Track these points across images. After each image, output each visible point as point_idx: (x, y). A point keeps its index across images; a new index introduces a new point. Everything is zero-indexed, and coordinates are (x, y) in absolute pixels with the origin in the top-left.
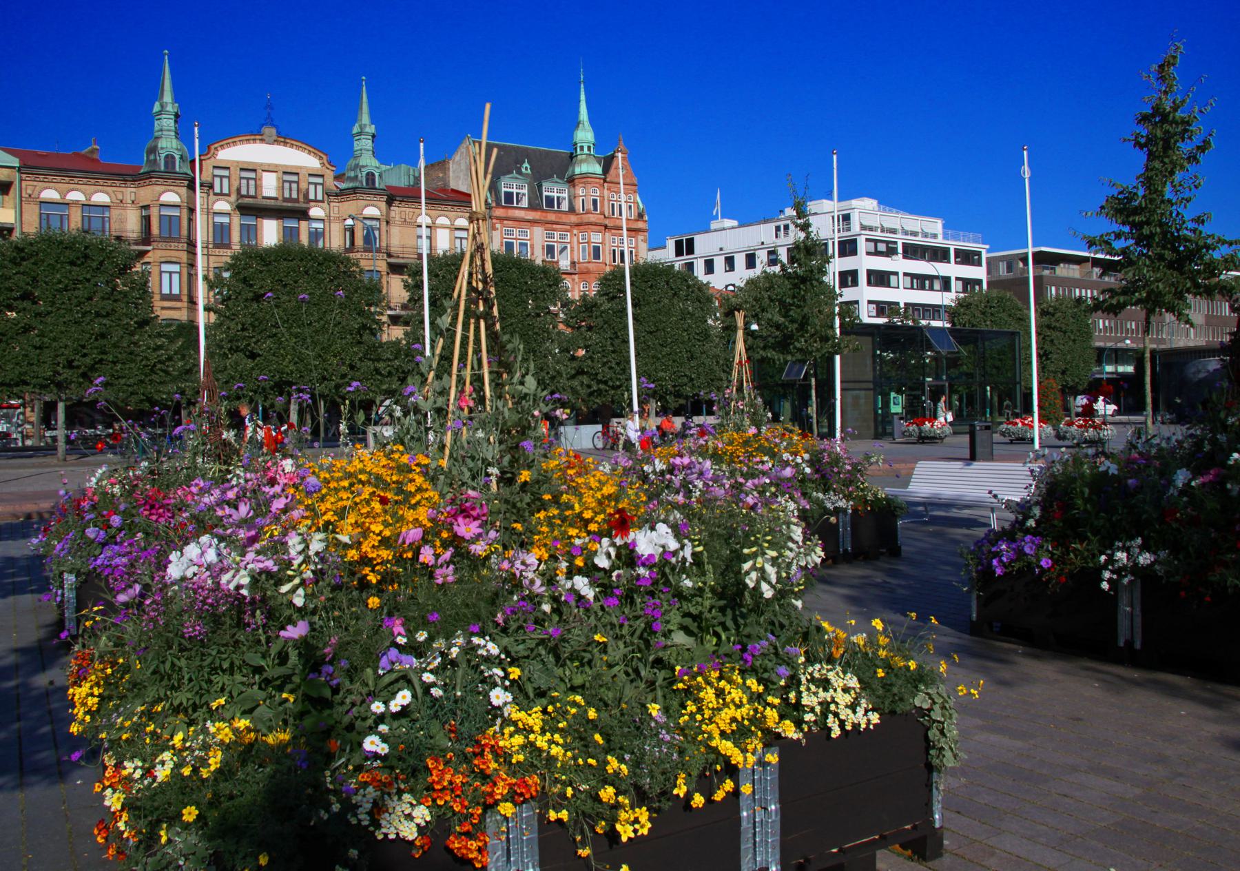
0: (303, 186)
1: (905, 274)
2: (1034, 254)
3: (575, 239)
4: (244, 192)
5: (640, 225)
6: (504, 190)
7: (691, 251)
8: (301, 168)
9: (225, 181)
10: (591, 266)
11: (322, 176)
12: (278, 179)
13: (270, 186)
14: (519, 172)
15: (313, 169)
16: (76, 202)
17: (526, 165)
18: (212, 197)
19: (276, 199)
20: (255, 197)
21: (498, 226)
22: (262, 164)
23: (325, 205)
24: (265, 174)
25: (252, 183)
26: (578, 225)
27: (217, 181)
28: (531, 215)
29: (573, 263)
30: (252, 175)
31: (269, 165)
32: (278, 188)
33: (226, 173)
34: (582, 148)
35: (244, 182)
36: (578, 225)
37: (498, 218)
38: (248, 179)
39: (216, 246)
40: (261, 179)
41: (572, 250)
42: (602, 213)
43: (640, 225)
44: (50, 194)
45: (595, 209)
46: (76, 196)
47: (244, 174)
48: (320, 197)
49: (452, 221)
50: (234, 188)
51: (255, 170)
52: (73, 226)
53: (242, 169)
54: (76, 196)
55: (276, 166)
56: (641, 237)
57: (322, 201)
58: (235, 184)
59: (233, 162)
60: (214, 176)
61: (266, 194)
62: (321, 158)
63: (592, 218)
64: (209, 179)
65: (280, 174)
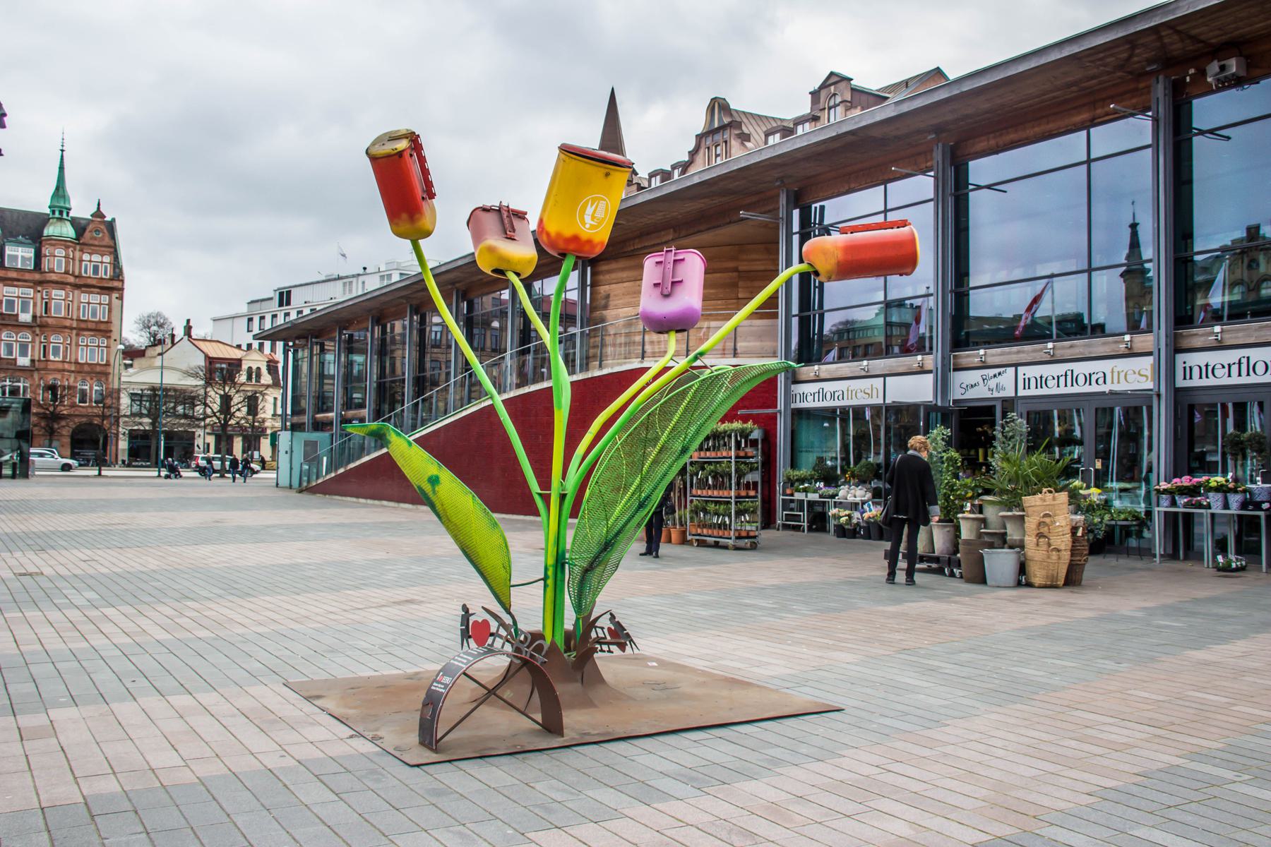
5: (116, 284)
7: (288, 303)
10: (50, 321)
26: (41, 283)
34: (54, 212)
36: (41, 283)
41: (35, 305)
43: (116, 284)
56: (115, 295)
63: (54, 277)
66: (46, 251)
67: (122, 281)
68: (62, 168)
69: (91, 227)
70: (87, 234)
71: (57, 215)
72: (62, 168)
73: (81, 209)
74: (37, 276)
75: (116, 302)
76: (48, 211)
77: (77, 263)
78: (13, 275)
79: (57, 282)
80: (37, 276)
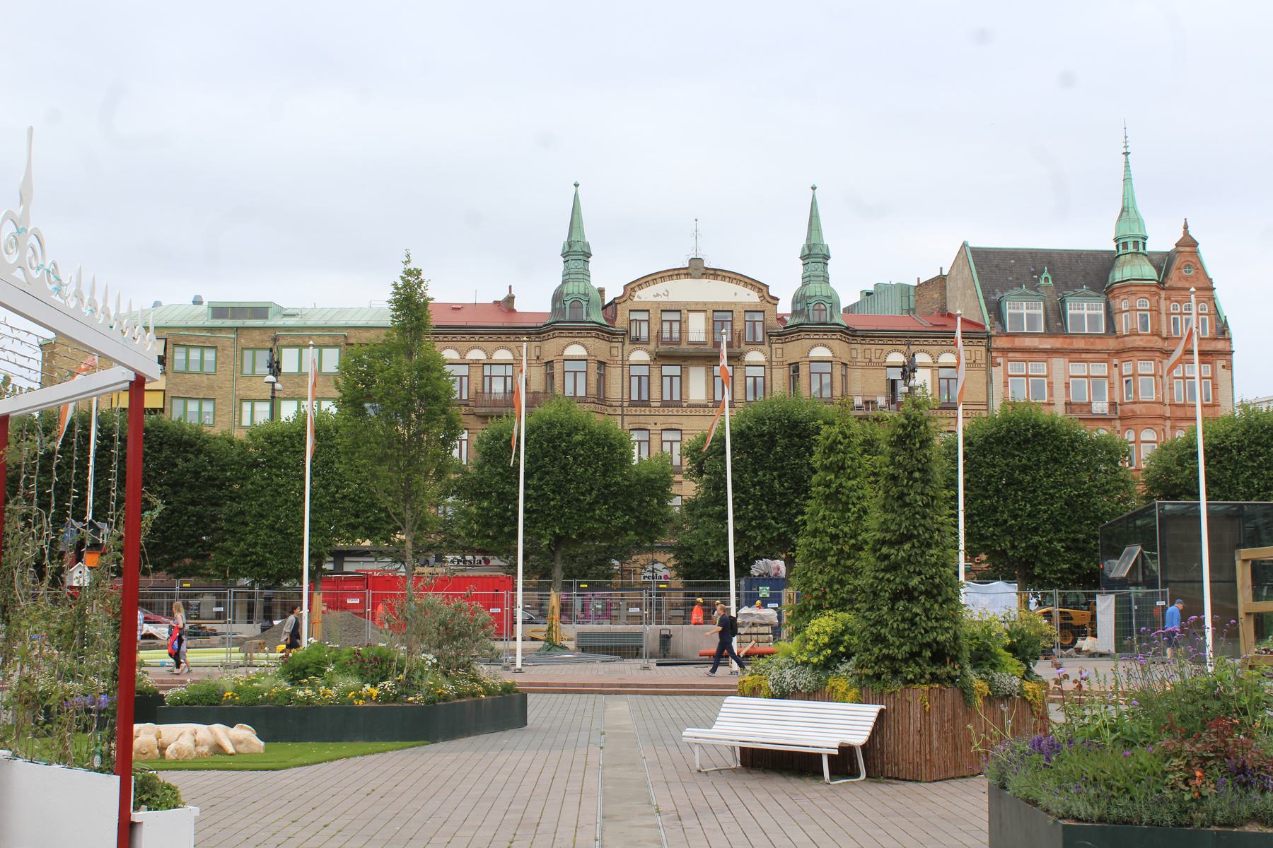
0: (739, 326)
2: (1089, 316)
3: (1116, 370)
4: (666, 335)
6: (1008, 311)
8: (735, 304)
9: (644, 326)
10: (1137, 408)
12: (707, 319)
13: (697, 329)
14: (1034, 286)
15: (750, 304)
17: (1046, 274)
18: (628, 347)
19: (704, 343)
20: (676, 343)
21: (1000, 360)
22: (688, 303)
23: (766, 348)
24: (691, 315)
25: (676, 326)
26: (1118, 352)
28: (1048, 344)
29: (1113, 405)
30: (676, 316)
31: (696, 303)
32: (707, 333)
33: (644, 316)
34: (1125, 245)
35: (666, 326)
36: (1118, 352)
37: (997, 349)
38: (671, 322)
39: (633, 404)
40: (686, 321)
42: (1157, 334)
43: (1220, 345)
45: (1145, 327)
47: (666, 316)
48: (760, 339)
49: (935, 358)
50: (654, 334)
52: (472, 388)
55: (705, 304)
56: (1220, 363)
57: (762, 343)
58: (655, 328)
61: (691, 339)
62: (760, 290)
63: (1138, 342)
64: (625, 325)
65: (710, 314)
66: (1122, 304)
67: (1230, 339)
68: (1127, 179)
69: (1177, 263)
70: (1174, 274)
71: (1131, 248)
72: (1127, 179)
73: (1162, 240)
74: (1112, 344)
75: (1222, 373)
76: (1112, 247)
77: (1164, 317)
78: (1080, 344)
79: (1144, 350)
80: (1112, 344)
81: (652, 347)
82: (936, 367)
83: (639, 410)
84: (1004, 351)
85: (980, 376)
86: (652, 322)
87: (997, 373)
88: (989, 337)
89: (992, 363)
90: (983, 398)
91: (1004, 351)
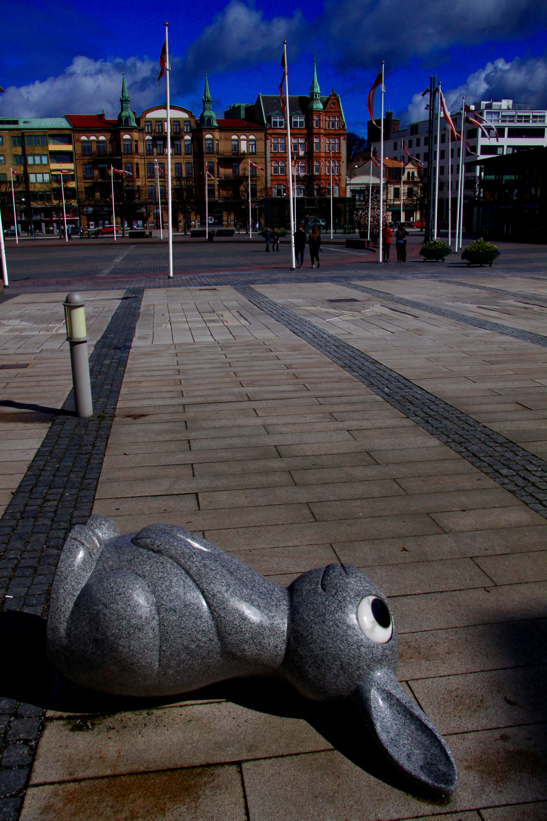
0: (182, 126)
1: (508, 147)
11: (190, 121)
16: (94, 140)
21: (269, 137)
27: (146, 127)
39: (147, 155)
44: (84, 138)
46: (93, 138)
51: (162, 121)
53: (156, 121)
54: (93, 138)
57: (189, 132)
59: (153, 118)
60: (145, 125)
62: (188, 114)
77: (324, 122)
81: (153, 134)
82: (248, 140)
83: (188, 156)
84: (271, 134)
85: (263, 143)
86: (153, 125)
87: (268, 142)
88: (266, 129)
89: (266, 139)
90: (264, 151)
91: (271, 134)
